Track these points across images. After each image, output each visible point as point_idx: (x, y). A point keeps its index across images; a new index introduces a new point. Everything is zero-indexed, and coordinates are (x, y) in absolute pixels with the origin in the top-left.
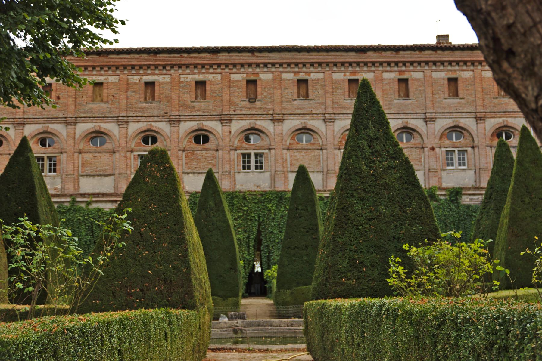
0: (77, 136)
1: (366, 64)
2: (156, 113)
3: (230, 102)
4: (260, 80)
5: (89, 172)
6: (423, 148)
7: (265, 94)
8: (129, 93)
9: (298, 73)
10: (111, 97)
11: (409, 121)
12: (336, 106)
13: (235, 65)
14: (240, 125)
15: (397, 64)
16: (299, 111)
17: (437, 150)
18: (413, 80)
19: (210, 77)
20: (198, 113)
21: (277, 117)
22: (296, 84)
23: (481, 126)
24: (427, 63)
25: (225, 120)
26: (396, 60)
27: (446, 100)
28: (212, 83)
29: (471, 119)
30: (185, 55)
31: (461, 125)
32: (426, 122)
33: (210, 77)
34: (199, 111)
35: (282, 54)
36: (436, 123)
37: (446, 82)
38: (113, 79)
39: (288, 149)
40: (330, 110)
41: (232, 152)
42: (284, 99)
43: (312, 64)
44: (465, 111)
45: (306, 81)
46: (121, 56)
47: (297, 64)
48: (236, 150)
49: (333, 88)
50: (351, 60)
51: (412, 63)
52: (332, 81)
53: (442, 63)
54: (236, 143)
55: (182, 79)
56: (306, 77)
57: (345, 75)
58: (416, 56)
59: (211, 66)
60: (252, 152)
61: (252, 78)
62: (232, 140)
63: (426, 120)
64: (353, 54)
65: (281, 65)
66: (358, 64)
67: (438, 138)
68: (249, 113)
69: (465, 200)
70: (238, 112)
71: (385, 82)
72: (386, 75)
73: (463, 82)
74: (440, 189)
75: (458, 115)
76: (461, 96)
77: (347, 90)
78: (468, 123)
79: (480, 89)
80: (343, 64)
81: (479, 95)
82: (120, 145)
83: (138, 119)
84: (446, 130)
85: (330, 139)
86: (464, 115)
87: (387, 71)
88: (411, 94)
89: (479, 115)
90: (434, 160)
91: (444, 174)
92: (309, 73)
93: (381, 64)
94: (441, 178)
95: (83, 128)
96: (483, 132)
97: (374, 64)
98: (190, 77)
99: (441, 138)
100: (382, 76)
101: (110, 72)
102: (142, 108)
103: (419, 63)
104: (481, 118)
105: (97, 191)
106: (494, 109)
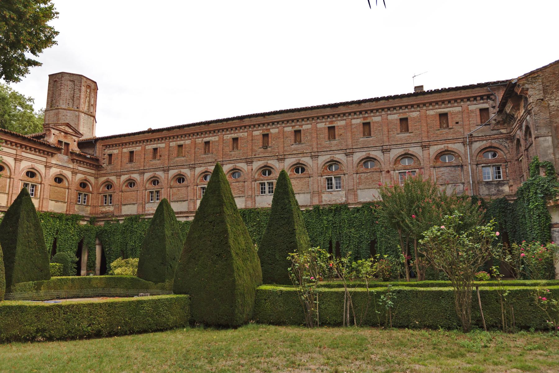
0: (121, 181)
1: (339, 115)
2: (210, 160)
3: (252, 150)
4: (271, 133)
5: (175, 199)
6: (381, 171)
7: (274, 142)
8: (196, 150)
9: (295, 126)
10: (186, 153)
11: (371, 153)
12: (319, 146)
13: (254, 126)
14: (258, 164)
15: (361, 112)
16: (295, 152)
17: (392, 172)
18: (373, 123)
19: (241, 135)
20: (234, 159)
21: (281, 157)
22: (293, 134)
23: (426, 152)
24: (383, 109)
25: (249, 162)
26: (360, 110)
27: (399, 135)
28: (213, 142)
29: (418, 148)
30: (225, 123)
31: (410, 152)
32: (383, 152)
33: (241, 135)
34: (234, 157)
35: (282, 115)
36: (391, 153)
37: (398, 122)
38: (188, 142)
40: (315, 150)
41: (253, 183)
42: (285, 145)
43: (303, 119)
44: (413, 142)
45: (299, 131)
46: (190, 128)
47: (293, 121)
48: (255, 181)
49: (317, 134)
50: (328, 114)
51: (372, 111)
52: (317, 130)
53: (395, 108)
54: (256, 176)
55: (225, 138)
57: (325, 124)
58: (374, 106)
59: (241, 127)
60: (266, 182)
61: (266, 132)
62: (253, 174)
63: (383, 151)
64: (328, 109)
65: (283, 122)
67: (392, 163)
68: (264, 156)
70: (257, 156)
71: (353, 127)
72: (354, 121)
73: (411, 120)
75: (408, 145)
76: (410, 131)
77: (327, 134)
78: (416, 150)
80: (323, 117)
81: (425, 129)
82: (191, 182)
84: (399, 157)
85: (315, 170)
86: (412, 145)
87: (355, 119)
88: (372, 133)
89: (424, 144)
90: (389, 180)
92: (301, 126)
93: (350, 114)
95: (172, 173)
96: (428, 156)
97: (344, 114)
98: (229, 136)
99: (395, 164)
100: (351, 122)
101: (186, 138)
102: (203, 158)
103: (377, 110)
104: (425, 147)
105: (179, 211)
106: (437, 139)
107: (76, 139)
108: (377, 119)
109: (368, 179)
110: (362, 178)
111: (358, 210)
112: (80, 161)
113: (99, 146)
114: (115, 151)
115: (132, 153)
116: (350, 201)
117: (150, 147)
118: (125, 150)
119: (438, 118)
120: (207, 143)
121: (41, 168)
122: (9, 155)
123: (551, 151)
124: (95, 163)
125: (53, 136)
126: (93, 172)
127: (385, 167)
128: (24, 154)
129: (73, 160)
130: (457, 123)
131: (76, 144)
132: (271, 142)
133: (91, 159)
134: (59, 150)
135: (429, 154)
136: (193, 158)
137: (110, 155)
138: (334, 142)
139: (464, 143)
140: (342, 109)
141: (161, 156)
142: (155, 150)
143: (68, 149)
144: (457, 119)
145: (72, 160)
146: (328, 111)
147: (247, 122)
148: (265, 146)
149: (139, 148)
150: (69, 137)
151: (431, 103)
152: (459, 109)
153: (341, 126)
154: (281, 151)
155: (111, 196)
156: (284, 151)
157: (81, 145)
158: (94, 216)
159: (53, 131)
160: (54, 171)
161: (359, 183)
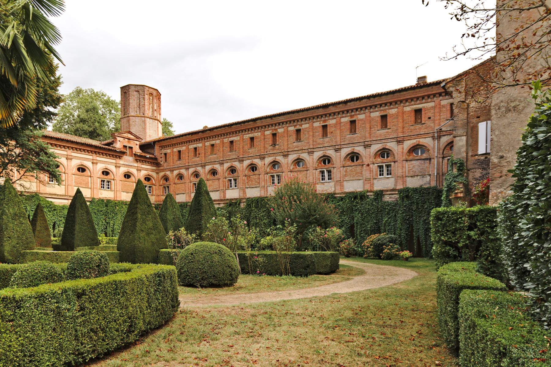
12: (315, 143)
15: (348, 111)
16: (296, 149)
17: (371, 166)
18: (358, 120)
21: (285, 153)
23: (400, 146)
24: (366, 108)
25: (262, 158)
26: (346, 109)
31: (387, 147)
39: (291, 172)
40: (311, 147)
42: (289, 143)
50: (321, 114)
51: (357, 109)
52: (313, 128)
53: (376, 106)
54: (268, 170)
56: (300, 128)
58: (357, 105)
60: (275, 174)
61: (274, 132)
64: (321, 110)
66: (326, 115)
69: (387, 198)
70: (268, 153)
71: (342, 125)
72: (343, 120)
74: (371, 191)
75: (385, 141)
79: (401, 121)
80: (318, 117)
81: (401, 125)
83: (227, 161)
85: (311, 164)
88: (357, 130)
91: (375, 181)
92: (301, 125)
93: (339, 113)
94: (373, 184)
95: (208, 168)
97: (334, 113)
103: (361, 109)
107: (138, 143)
108: (362, 117)
109: (352, 172)
110: (348, 170)
111: (342, 199)
112: (143, 161)
113: (157, 147)
114: (169, 151)
115: (180, 152)
116: (337, 192)
117: (192, 147)
118: (175, 150)
119: (413, 113)
120: (232, 142)
121: (112, 168)
122: (87, 160)
123: (464, 149)
124: (155, 162)
125: (119, 143)
126: (154, 168)
127: (366, 161)
128: (98, 158)
129: (137, 161)
130: (430, 118)
131: (138, 147)
132: (279, 140)
133: (150, 158)
134: (124, 153)
135: (403, 148)
136: (221, 155)
137: (165, 154)
138: (326, 140)
139: (433, 138)
140: (332, 109)
141: (199, 154)
142: (195, 149)
143: (132, 152)
144: (430, 115)
145: (136, 160)
146: (321, 112)
147: (259, 123)
148: (274, 144)
149: (184, 148)
150: (132, 142)
151: (407, 100)
152: (432, 104)
153: (332, 124)
154: (286, 147)
155: (168, 187)
156: (288, 148)
157: (142, 147)
158: (158, 203)
159: (118, 139)
160: (123, 170)
161: (346, 176)
